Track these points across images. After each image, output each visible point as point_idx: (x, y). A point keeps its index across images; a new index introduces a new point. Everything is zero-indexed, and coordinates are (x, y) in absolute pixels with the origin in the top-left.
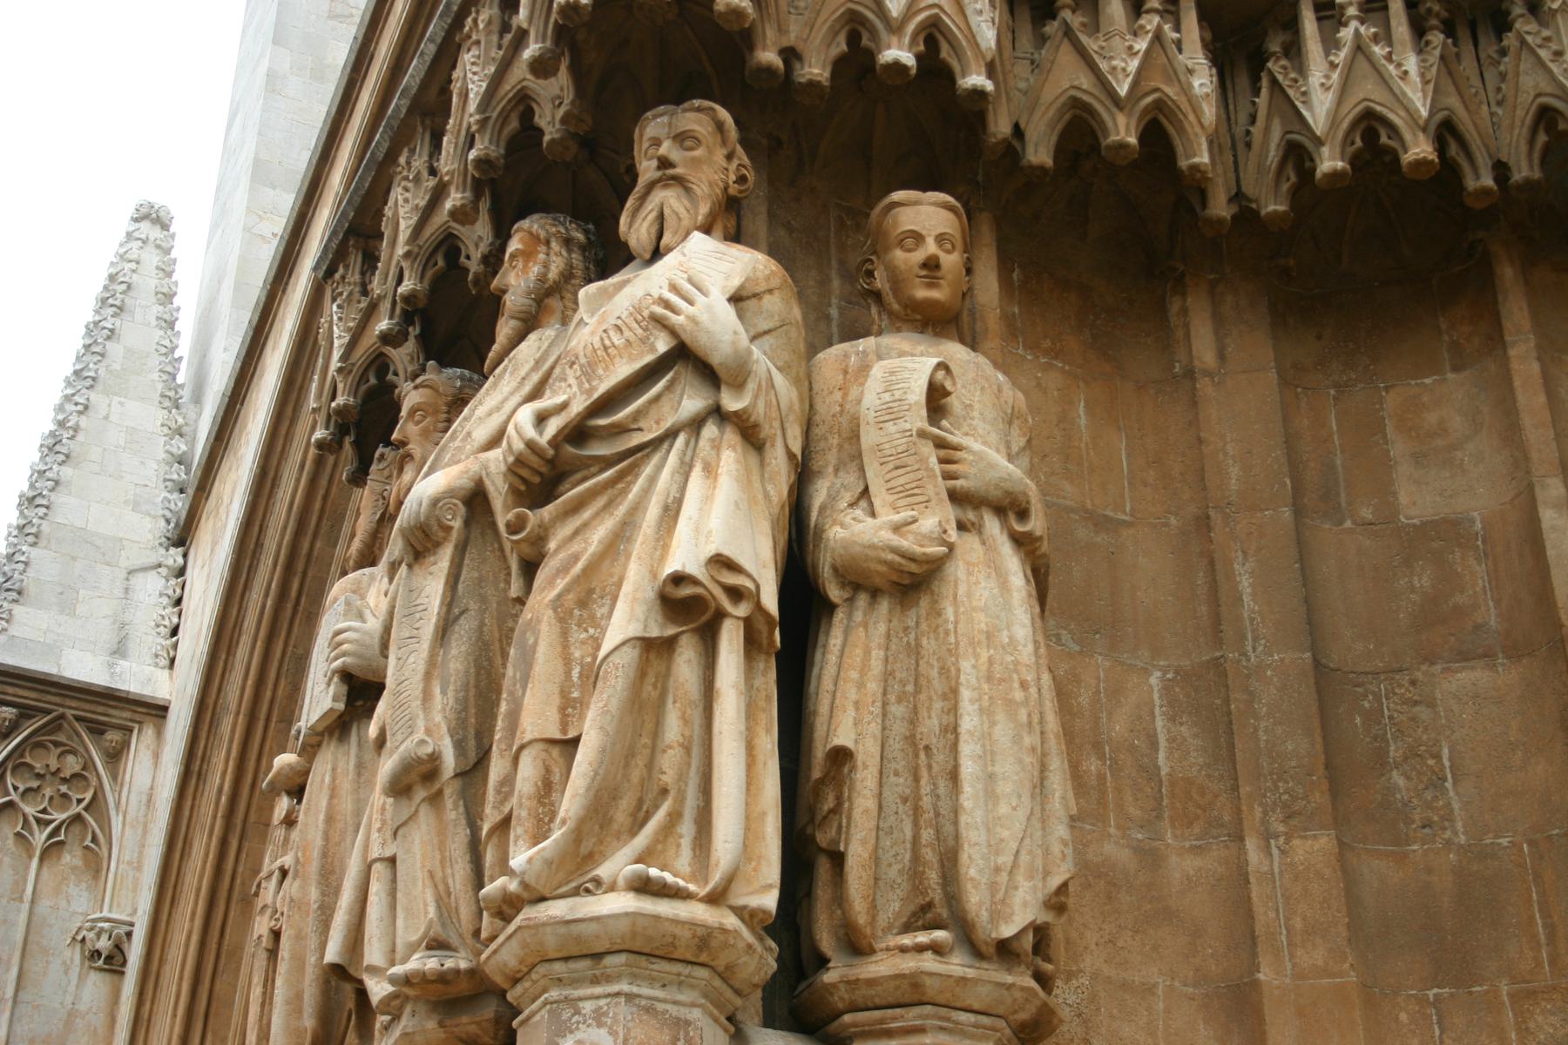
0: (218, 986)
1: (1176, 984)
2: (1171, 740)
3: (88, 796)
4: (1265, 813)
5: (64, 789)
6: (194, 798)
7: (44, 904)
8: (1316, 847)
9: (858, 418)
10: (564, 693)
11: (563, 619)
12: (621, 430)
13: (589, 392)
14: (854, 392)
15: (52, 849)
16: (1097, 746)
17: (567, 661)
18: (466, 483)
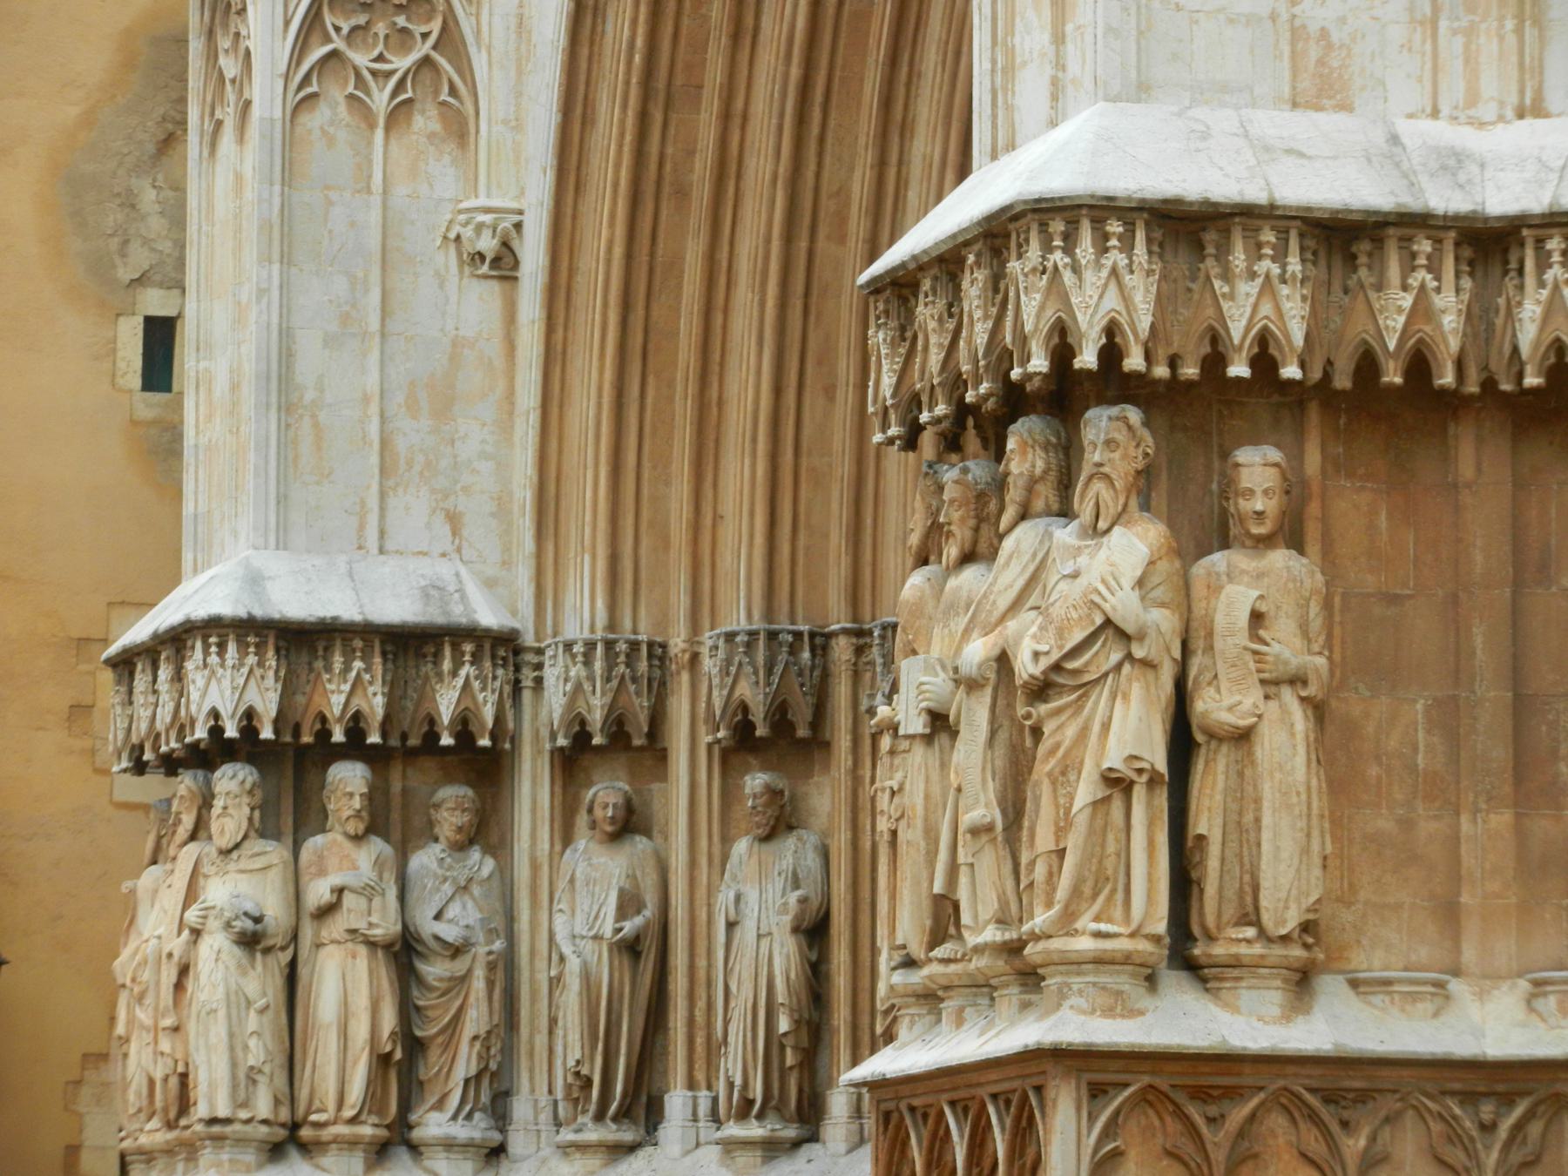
0: (656, 312)
1: (1418, 901)
2: (1427, 746)
3: (435, 26)
4: (1476, 797)
5: (401, 21)
6: (592, 44)
7: (400, 191)
8: (1502, 820)
9: (1212, 629)
10: (1056, 824)
11: (1054, 783)
12: (1076, 672)
13: (1061, 647)
14: (1213, 601)
15: (400, 113)
16: (1378, 758)
17: (1057, 806)
18: (996, 652)
